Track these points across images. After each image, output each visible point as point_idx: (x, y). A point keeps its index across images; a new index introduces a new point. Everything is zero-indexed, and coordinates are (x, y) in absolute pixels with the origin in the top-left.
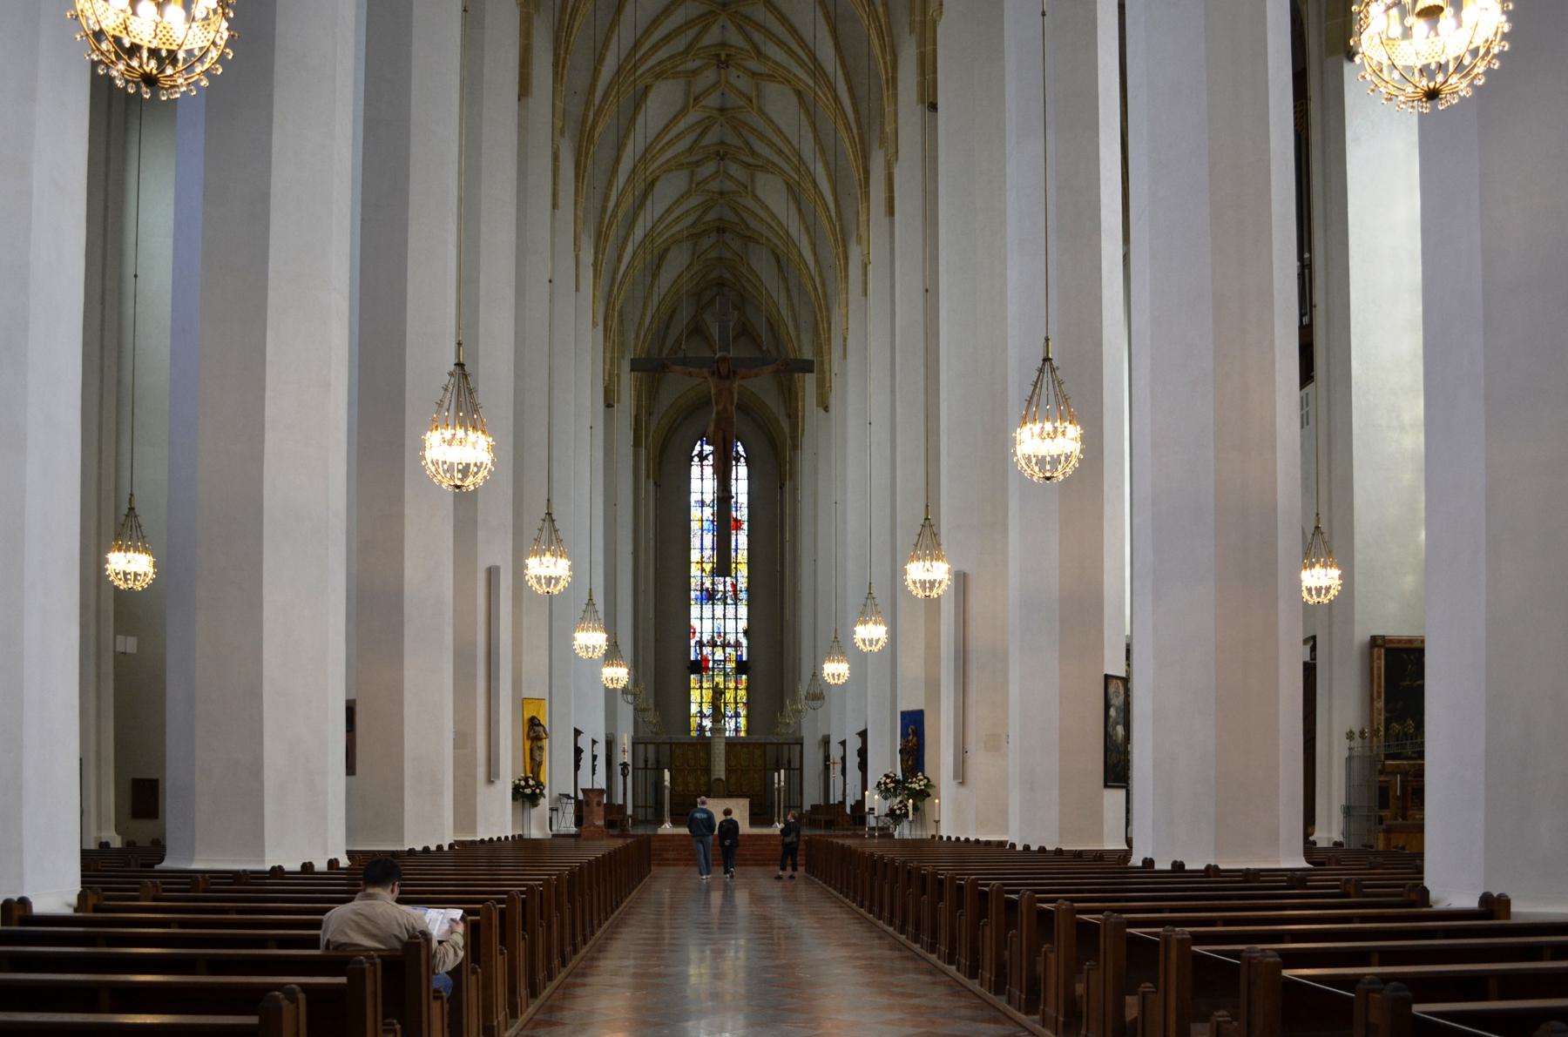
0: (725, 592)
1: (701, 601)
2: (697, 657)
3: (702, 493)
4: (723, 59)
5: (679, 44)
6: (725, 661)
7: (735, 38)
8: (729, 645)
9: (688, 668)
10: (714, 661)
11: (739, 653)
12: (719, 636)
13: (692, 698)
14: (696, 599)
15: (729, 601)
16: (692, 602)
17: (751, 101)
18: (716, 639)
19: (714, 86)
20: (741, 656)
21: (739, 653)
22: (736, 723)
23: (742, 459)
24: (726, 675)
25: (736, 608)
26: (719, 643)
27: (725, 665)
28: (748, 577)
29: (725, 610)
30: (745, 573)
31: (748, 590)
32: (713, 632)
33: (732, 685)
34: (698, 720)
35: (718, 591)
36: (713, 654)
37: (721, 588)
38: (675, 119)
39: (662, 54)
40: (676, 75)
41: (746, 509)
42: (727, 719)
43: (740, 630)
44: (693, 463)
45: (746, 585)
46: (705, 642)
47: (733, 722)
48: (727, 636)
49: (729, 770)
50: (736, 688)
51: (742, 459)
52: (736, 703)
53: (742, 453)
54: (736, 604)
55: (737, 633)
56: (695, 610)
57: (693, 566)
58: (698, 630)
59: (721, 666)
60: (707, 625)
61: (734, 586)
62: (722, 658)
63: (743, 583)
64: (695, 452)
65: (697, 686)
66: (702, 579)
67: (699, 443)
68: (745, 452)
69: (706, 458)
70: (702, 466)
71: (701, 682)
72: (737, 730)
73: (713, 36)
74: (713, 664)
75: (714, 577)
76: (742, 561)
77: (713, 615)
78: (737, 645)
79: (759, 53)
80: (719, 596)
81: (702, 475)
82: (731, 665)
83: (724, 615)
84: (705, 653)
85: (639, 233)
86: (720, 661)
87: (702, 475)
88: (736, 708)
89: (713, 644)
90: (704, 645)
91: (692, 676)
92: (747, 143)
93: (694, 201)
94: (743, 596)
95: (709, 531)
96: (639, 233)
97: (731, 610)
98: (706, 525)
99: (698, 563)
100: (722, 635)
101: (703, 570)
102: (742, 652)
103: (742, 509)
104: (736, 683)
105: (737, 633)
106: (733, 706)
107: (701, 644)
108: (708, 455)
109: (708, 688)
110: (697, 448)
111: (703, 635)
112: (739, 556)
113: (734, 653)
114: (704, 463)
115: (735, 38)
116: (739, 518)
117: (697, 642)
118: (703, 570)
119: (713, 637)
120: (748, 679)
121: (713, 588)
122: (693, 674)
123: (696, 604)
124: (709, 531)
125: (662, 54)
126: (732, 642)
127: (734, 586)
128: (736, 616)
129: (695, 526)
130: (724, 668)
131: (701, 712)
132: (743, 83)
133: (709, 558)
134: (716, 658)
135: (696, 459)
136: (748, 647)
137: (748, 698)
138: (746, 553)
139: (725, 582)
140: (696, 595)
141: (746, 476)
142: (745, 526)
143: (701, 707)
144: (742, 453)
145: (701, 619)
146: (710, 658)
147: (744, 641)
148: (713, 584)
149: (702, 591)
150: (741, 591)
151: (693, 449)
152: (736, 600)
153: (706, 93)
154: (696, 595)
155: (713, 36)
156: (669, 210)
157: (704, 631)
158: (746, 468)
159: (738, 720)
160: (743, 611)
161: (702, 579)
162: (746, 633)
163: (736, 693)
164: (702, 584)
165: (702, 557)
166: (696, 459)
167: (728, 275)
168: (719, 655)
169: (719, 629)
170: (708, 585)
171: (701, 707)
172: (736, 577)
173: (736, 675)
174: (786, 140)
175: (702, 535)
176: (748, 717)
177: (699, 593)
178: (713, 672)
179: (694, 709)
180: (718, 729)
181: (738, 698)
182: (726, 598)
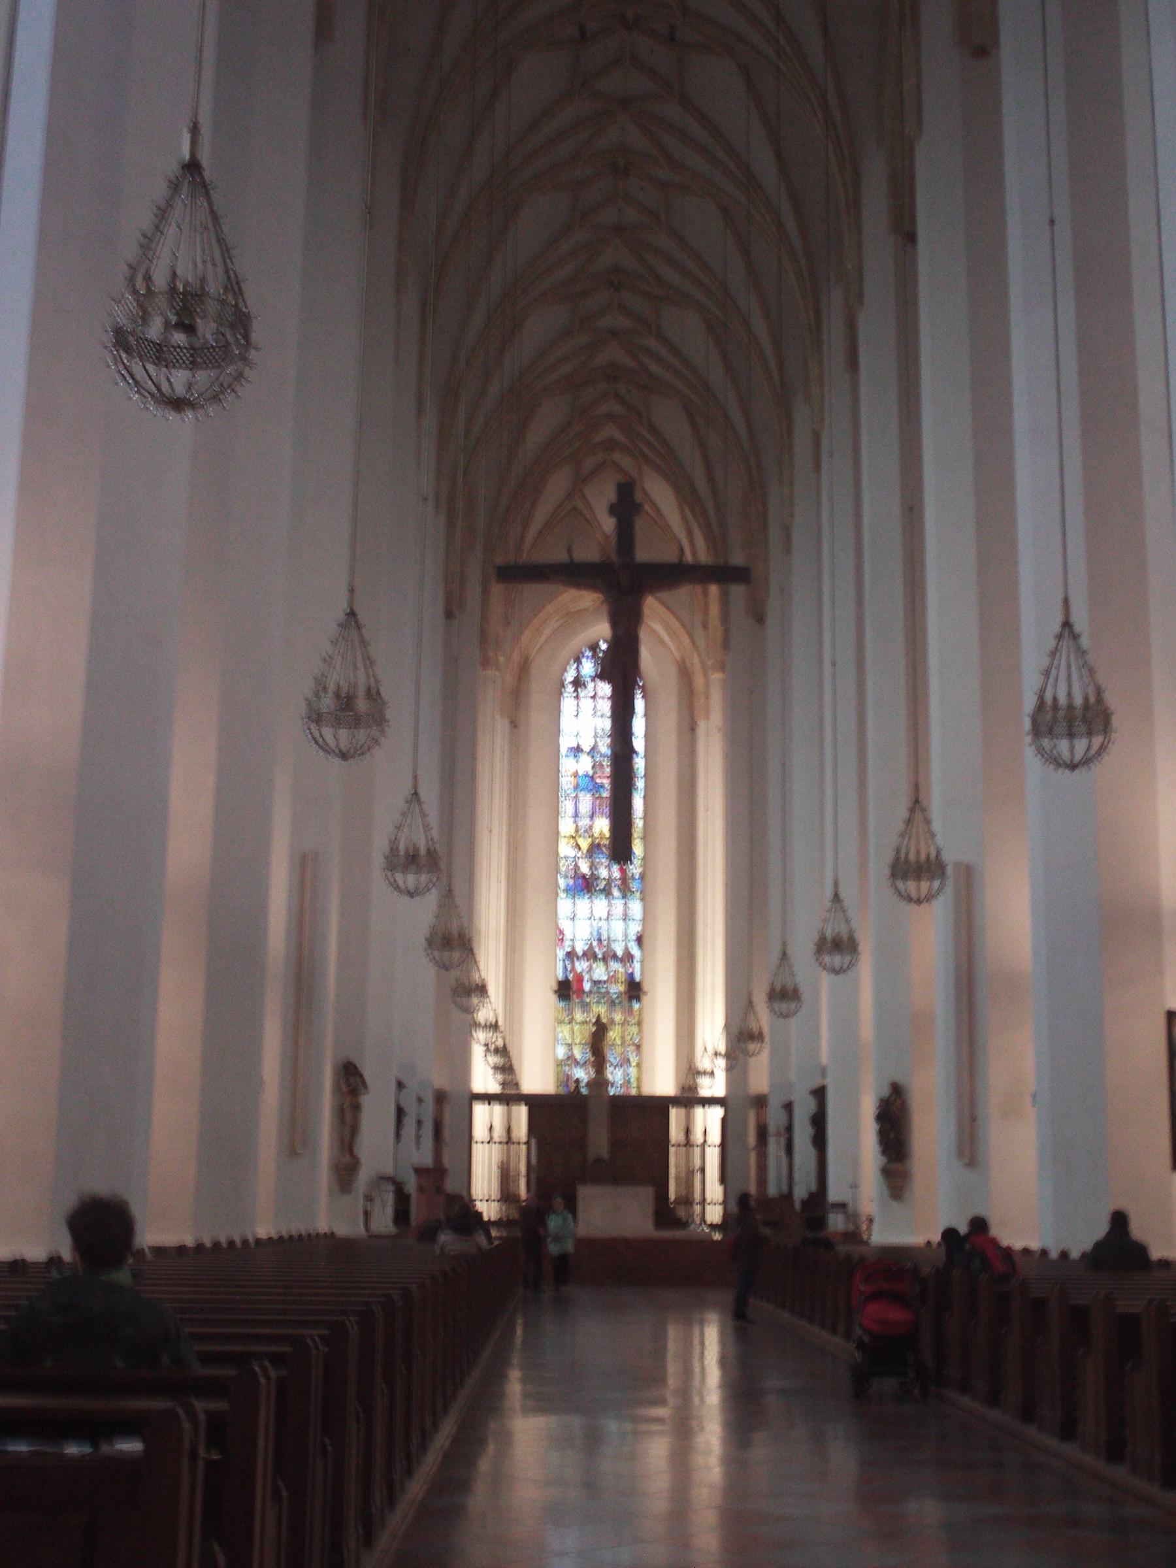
0: (609, 881)
11: (630, 971)
18: (597, 950)
26: (600, 956)
36: (590, 969)
46: (580, 953)
49: (615, 1144)
78: (628, 957)
82: (617, 989)
89: (590, 955)
97: (618, 905)
107: (571, 955)
109: (585, 1022)
113: (621, 970)
134: (596, 977)
140: (568, 885)
147: (635, 951)
148: (593, 867)
150: (633, 878)
162: (640, 940)
163: (623, 1032)
165: (577, 831)
167: (618, 435)
168: (600, 972)
180: (599, 1082)
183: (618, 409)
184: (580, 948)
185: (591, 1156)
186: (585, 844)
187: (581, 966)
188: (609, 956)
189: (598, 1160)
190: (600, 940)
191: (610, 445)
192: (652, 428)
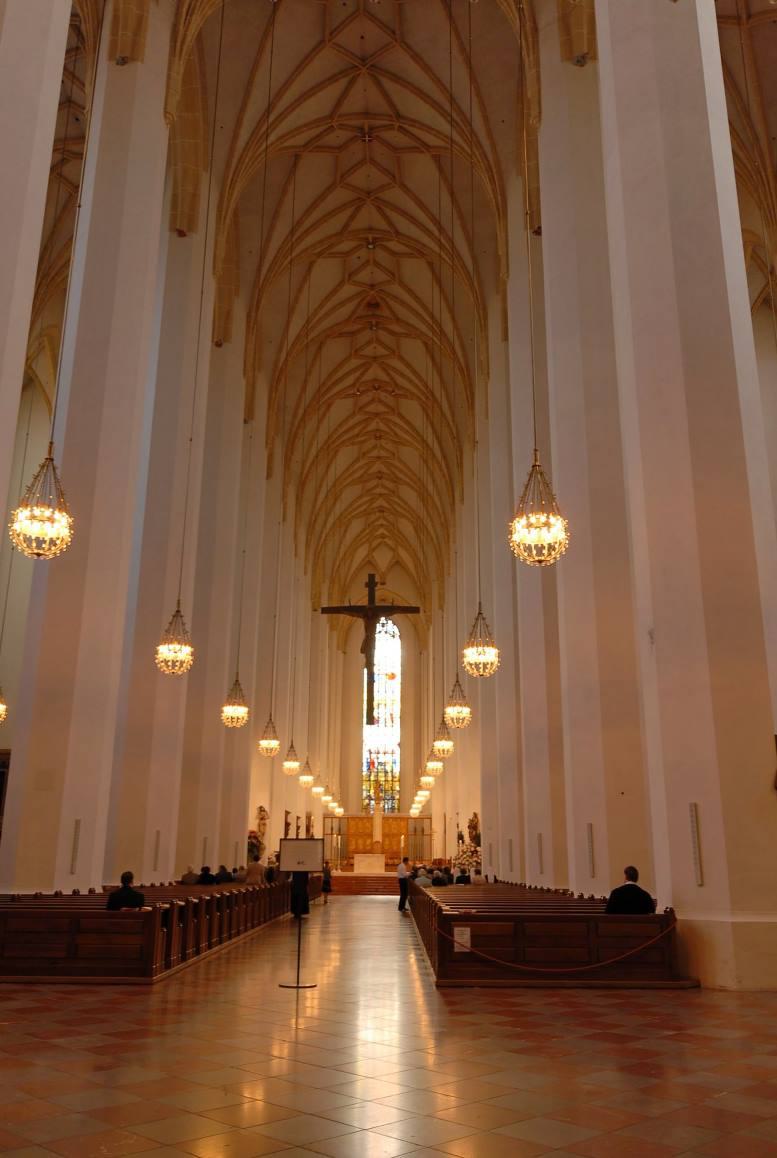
1: (368, 723)
4: (378, 435)
5: (356, 431)
7: (382, 426)
17: (394, 454)
19: (375, 447)
34: (367, 801)
38: (352, 464)
39: (345, 437)
40: (353, 444)
47: (390, 802)
49: (385, 835)
51: (397, 637)
72: (393, 808)
73: (373, 426)
79: (396, 434)
85: (331, 520)
92: (393, 473)
93: (365, 499)
96: (331, 520)
115: (382, 426)
125: (345, 437)
131: (369, 796)
132: (390, 446)
153: (368, 452)
155: (373, 426)
156: (351, 505)
174: (415, 475)
179: (365, 794)
183: (385, 523)
187: (374, 756)
191: (383, 536)
192: (398, 530)
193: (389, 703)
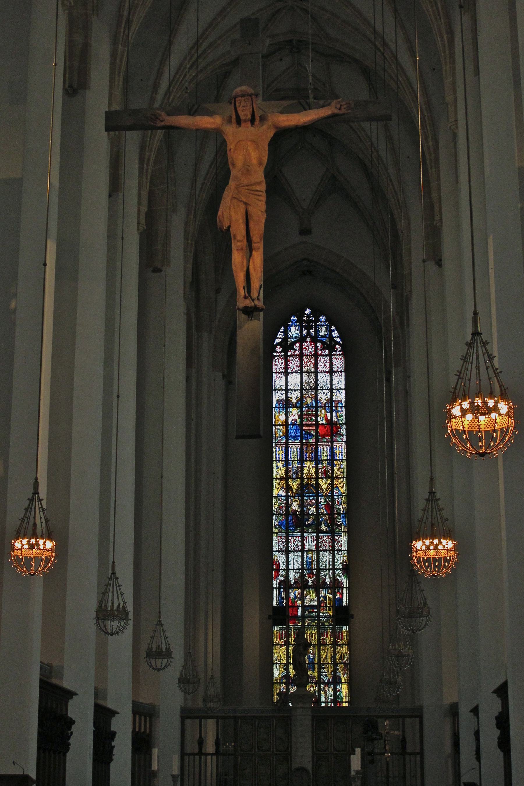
0: (318, 515)
2: (281, 603)
3: (287, 390)
6: (318, 607)
8: (324, 585)
9: (270, 617)
10: (304, 607)
11: (338, 596)
12: (311, 574)
13: (276, 656)
14: (280, 526)
15: (323, 528)
16: (276, 531)
20: (341, 599)
21: (338, 596)
22: (335, 691)
23: (337, 346)
24: (320, 626)
25: (333, 537)
27: (318, 612)
28: (348, 496)
29: (317, 540)
30: (344, 490)
31: (348, 512)
32: (303, 569)
33: (329, 639)
35: (308, 514)
36: (303, 598)
37: (312, 510)
41: (344, 409)
42: (322, 686)
43: (339, 565)
44: (275, 354)
45: (345, 506)
46: (292, 582)
48: (322, 574)
50: (335, 644)
51: (337, 346)
52: (335, 663)
53: (338, 340)
54: (333, 532)
55: (334, 569)
56: (278, 542)
57: (276, 482)
58: (283, 566)
59: (314, 614)
60: (295, 561)
61: (330, 507)
62: (316, 604)
63: (341, 506)
64: (278, 341)
65: (281, 642)
66: (287, 500)
67: (282, 329)
68: (341, 337)
69: (291, 347)
70: (286, 357)
71: (287, 636)
72: (336, 699)
74: (303, 612)
75: (302, 497)
76: (339, 475)
77: (303, 545)
78: (335, 585)
80: (310, 521)
81: (286, 367)
83: (317, 546)
84: (292, 596)
86: (313, 607)
87: (286, 367)
88: (335, 670)
89: (301, 584)
90: (291, 587)
91: (276, 629)
94: (342, 520)
95: (296, 438)
98: (292, 430)
99: (281, 479)
100: (314, 571)
101: (288, 488)
102: (341, 594)
103: (339, 409)
104: (335, 636)
105: (334, 569)
106: (330, 668)
107: (286, 585)
108: (294, 343)
110: (281, 335)
111: (291, 572)
112: (336, 469)
114: (289, 353)
116: (335, 419)
117: (281, 581)
118: (288, 488)
119: (302, 575)
120: (349, 632)
121: (302, 511)
122: (276, 623)
123: (280, 532)
124: (296, 438)
126: (328, 580)
127: (330, 507)
128: (333, 546)
129: (278, 432)
130: (318, 616)
133: (297, 472)
134: (307, 602)
135: (279, 349)
136: (349, 588)
137: (349, 659)
138: (344, 465)
139: (318, 503)
141: (342, 368)
142: (343, 431)
143: (287, 670)
144: (338, 340)
145: (287, 552)
146: (299, 603)
148: (302, 505)
149: (287, 515)
150: (339, 514)
151: (276, 337)
152: (333, 528)
154: (280, 521)
157: (291, 567)
158: (342, 357)
159: (338, 688)
160: (342, 541)
161: (287, 500)
162: (346, 569)
164: (288, 506)
165: (287, 471)
166: (279, 349)
168: (311, 599)
169: (310, 564)
170: (295, 506)
171: (287, 670)
172: (333, 496)
173: (334, 626)
175: (287, 443)
176: (349, 683)
177: (283, 518)
178: (303, 623)
179: (277, 672)
181: (338, 657)
182: (320, 524)
184: (292, 576)
185: (295, 766)
186: (295, 485)
188: (319, 585)
189: (303, 770)
190: (310, 570)
193: (324, 484)
